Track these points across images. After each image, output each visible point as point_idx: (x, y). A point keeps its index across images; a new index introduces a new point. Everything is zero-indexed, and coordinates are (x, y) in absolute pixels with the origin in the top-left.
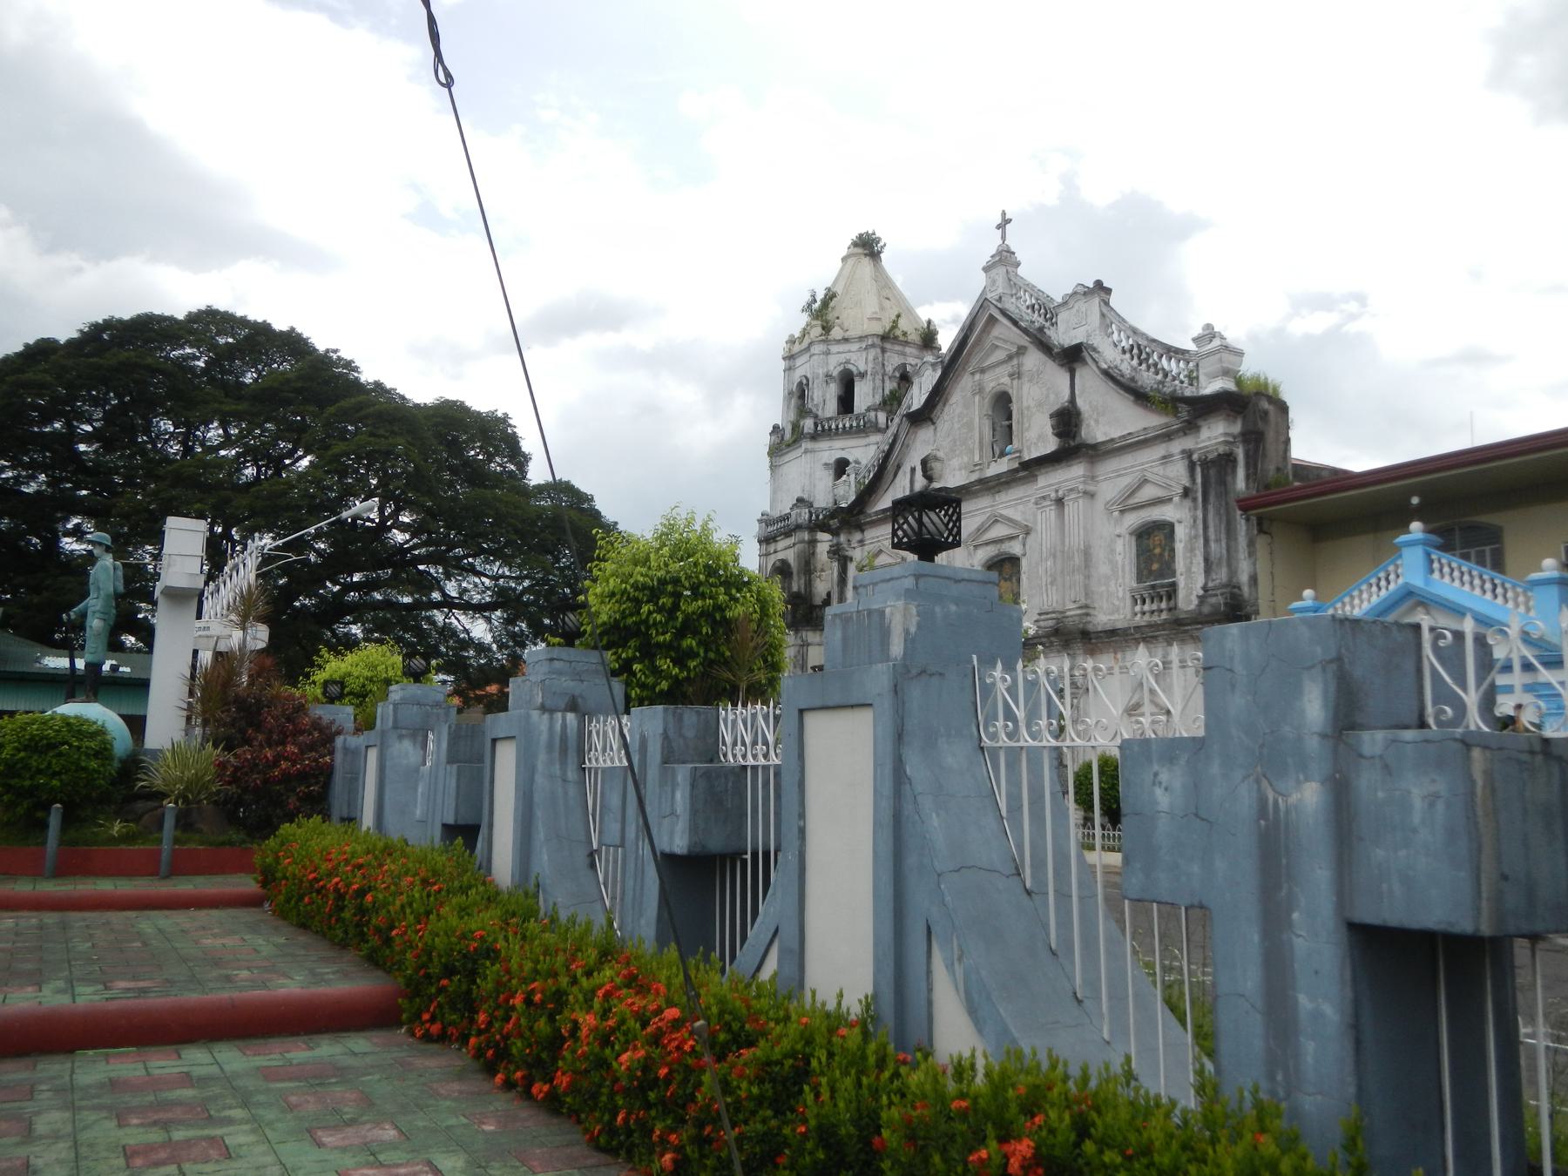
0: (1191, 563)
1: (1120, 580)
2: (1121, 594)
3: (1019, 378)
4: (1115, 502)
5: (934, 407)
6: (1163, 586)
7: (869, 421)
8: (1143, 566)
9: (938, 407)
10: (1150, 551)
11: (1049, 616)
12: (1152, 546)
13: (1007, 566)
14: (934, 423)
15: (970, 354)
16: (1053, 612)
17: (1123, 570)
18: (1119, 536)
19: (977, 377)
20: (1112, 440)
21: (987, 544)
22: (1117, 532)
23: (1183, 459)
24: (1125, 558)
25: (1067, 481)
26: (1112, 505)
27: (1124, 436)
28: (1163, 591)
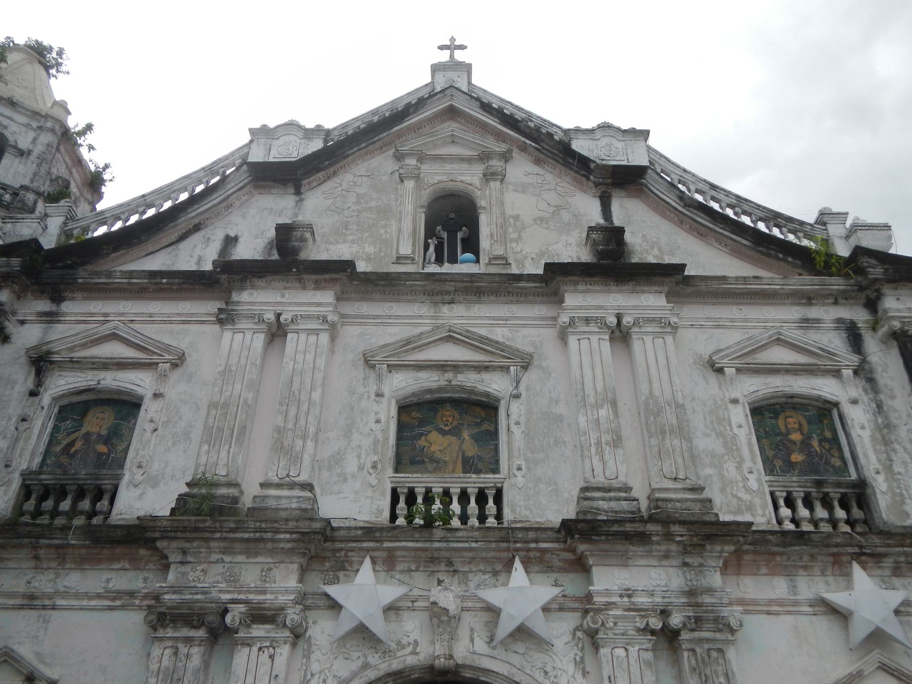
0: (891, 460)
1: (748, 464)
2: (753, 484)
3: (502, 181)
4: (727, 356)
5: (318, 170)
6: (839, 485)
7: (22, 201)
8: (770, 454)
9: (320, 175)
10: (780, 434)
11: (612, 494)
12: (784, 430)
13: (448, 415)
14: (298, 192)
15: (399, 135)
16: (619, 490)
17: (751, 451)
18: (735, 401)
19: (411, 162)
20: (724, 278)
21: (420, 367)
22: (735, 394)
23: (837, 329)
24: (750, 434)
25: (635, 307)
26: (722, 358)
27: (745, 278)
28: (835, 493)
